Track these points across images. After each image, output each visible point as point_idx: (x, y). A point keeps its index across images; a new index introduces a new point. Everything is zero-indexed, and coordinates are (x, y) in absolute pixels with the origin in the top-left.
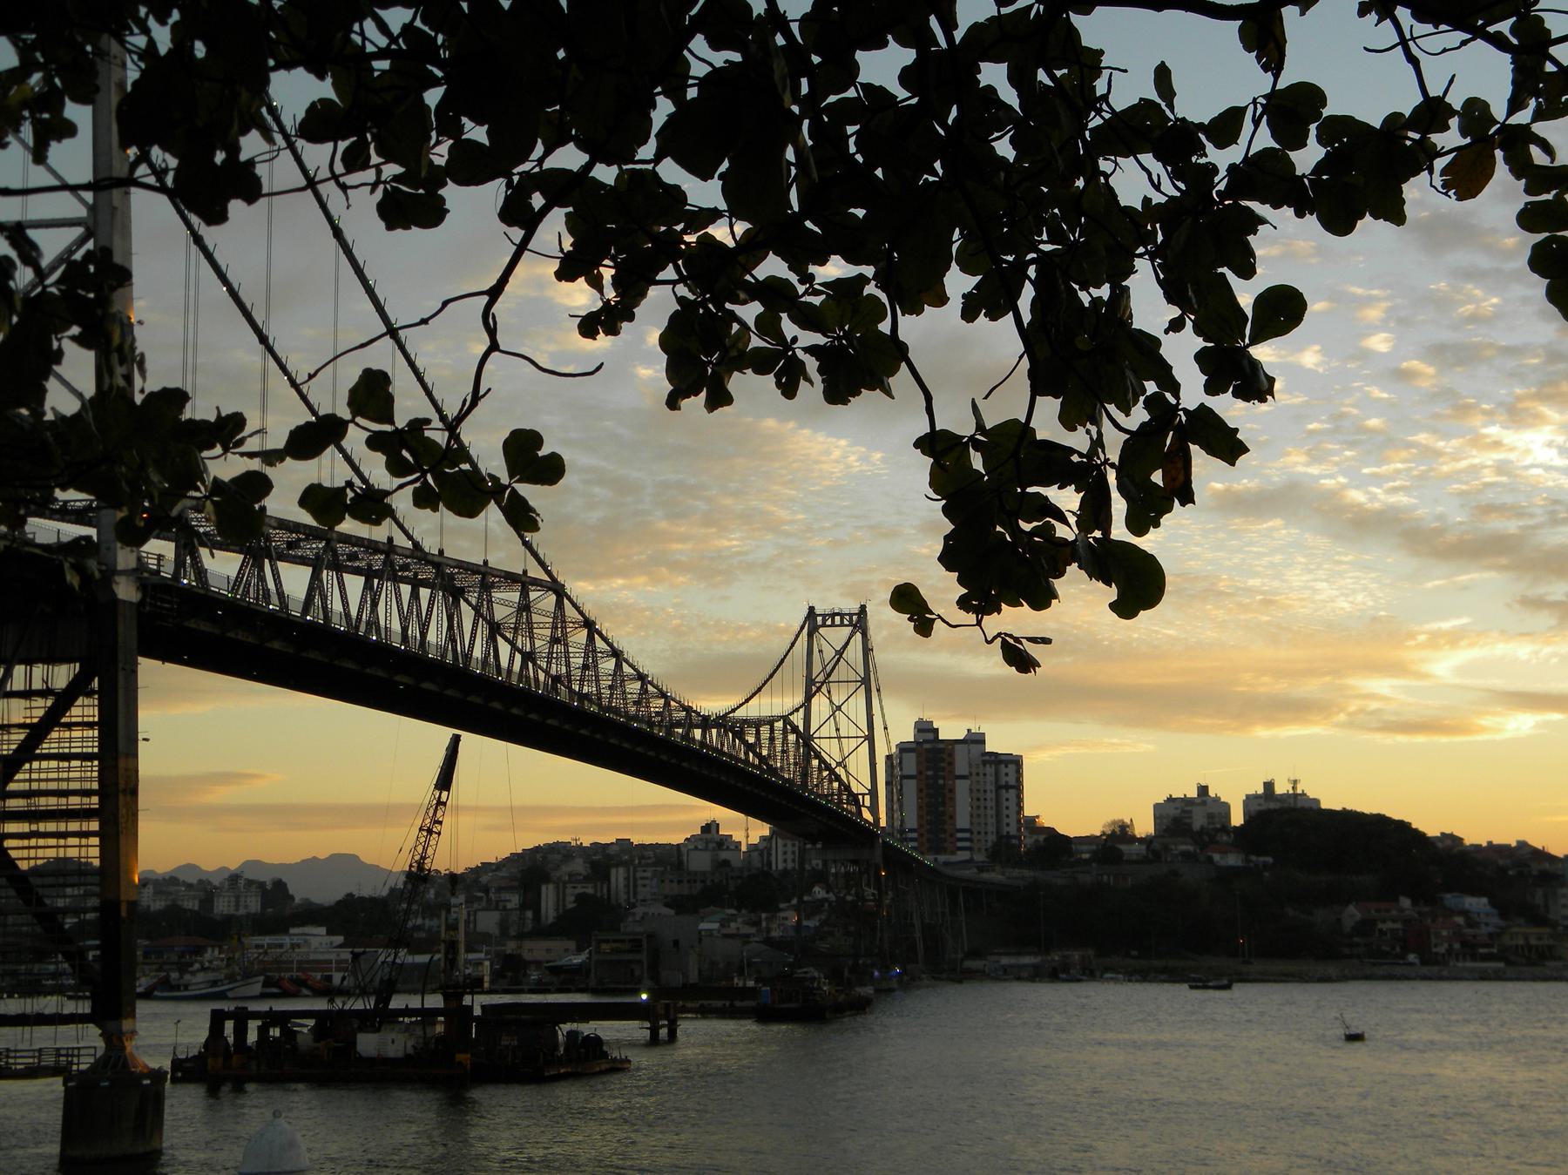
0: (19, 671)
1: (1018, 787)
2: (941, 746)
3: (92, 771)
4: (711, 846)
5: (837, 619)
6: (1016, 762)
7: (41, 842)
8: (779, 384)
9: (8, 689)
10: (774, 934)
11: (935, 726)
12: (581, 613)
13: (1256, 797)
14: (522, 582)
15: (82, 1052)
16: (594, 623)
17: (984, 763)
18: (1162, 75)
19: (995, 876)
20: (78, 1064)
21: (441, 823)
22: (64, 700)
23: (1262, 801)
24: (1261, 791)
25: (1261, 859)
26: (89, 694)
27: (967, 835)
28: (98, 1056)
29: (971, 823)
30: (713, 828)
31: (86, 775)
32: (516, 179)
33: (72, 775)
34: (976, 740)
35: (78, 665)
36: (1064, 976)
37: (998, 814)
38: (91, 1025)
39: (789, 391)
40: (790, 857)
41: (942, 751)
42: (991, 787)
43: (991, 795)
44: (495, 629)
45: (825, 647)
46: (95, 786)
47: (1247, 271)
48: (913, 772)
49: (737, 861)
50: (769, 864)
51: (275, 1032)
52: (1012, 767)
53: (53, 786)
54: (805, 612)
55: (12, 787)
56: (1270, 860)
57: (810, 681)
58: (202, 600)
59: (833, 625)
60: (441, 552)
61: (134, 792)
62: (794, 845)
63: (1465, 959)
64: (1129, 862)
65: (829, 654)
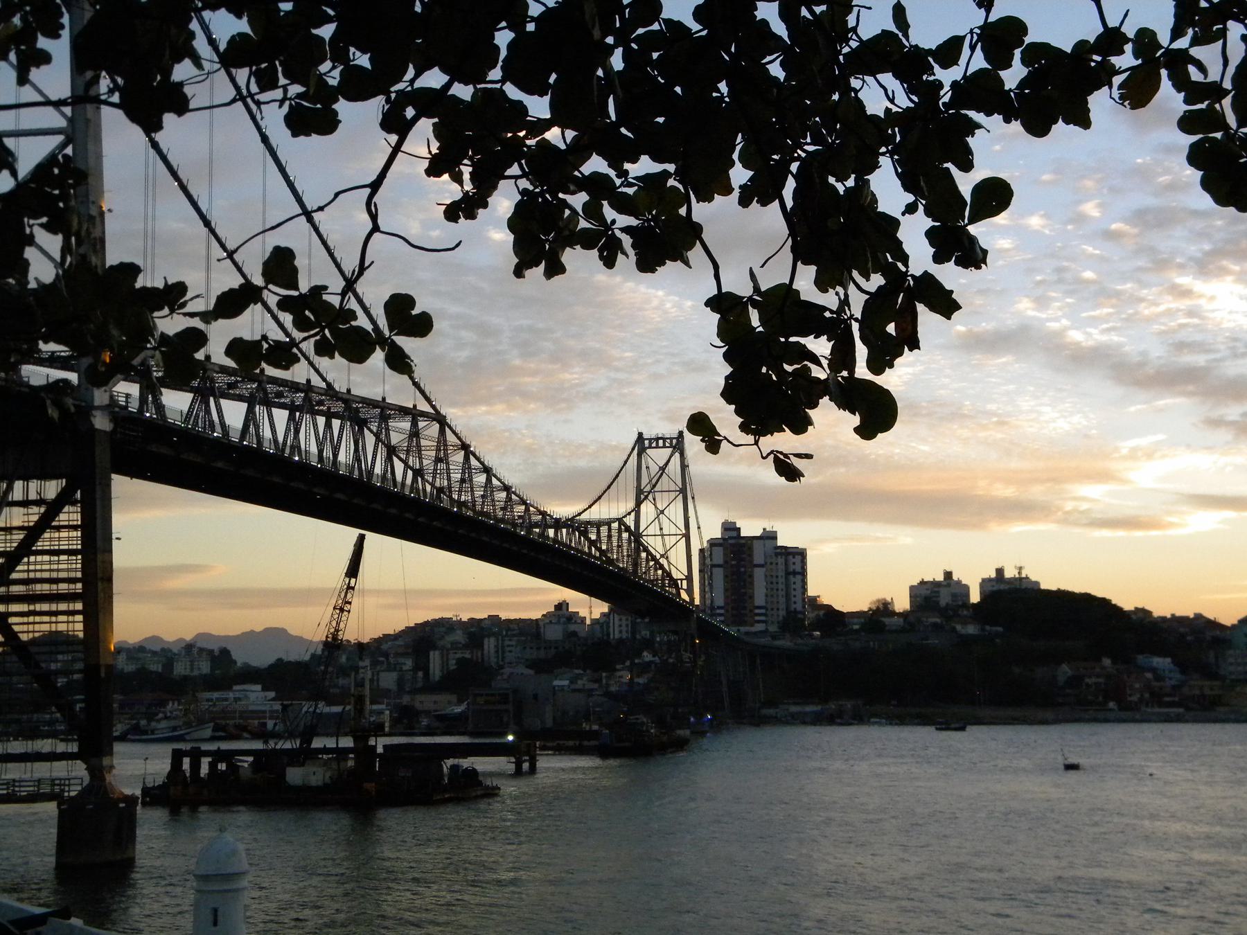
0: (18, 485)
1: (803, 573)
2: (743, 541)
3: (76, 563)
4: (563, 620)
5: (661, 442)
6: (801, 554)
7: (38, 619)
8: (601, 257)
9: (10, 499)
10: (613, 689)
11: (738, 526)
12: (459, 438)
13: (990, 580)
14: (413, 414)
15: (72, 782)
16: (469, 446)
17: (777, 555)
18: (899, 13)
19: (786, 643)
20: (69, 791)
21: (350, 603)
22: (54, 508)
23: (994, 583)
24: (993, 575)
25: (994, 629)
26: (74, 503)
27: (763, 611)
28: (85, 784)
29: (766, 602)
30: (564, 607)
31: (72, 566)
32: (393, 96)
33: (61, 567)
34: (770, 536)
35: (64, 480)
36: (839, 721)
37: (787, 596)
38: (78, 762)
39: (609, 262)
40: (624, 628)
41: (743, 545)
42: (781, 573)
43: (781, 580)
44: (392, 451)
45: (651, 463)
46: (79, 575)
47: (967, 166)
48: (721, 562)
49: (582, 634)
50: (608, 635)
51: (222, 766)
52: (798, 558)
53: (46, 575)
54: (635, 436)
55: (14, 576)
56: (1000, 629)
57: (639, 491)
58: (161, 429)
59: (657, 447)
60: (349, 391)
61: (109, 580)
62: (627, 620)
63: (1153, 706)
64: (891, 632)
65: (654, 469)
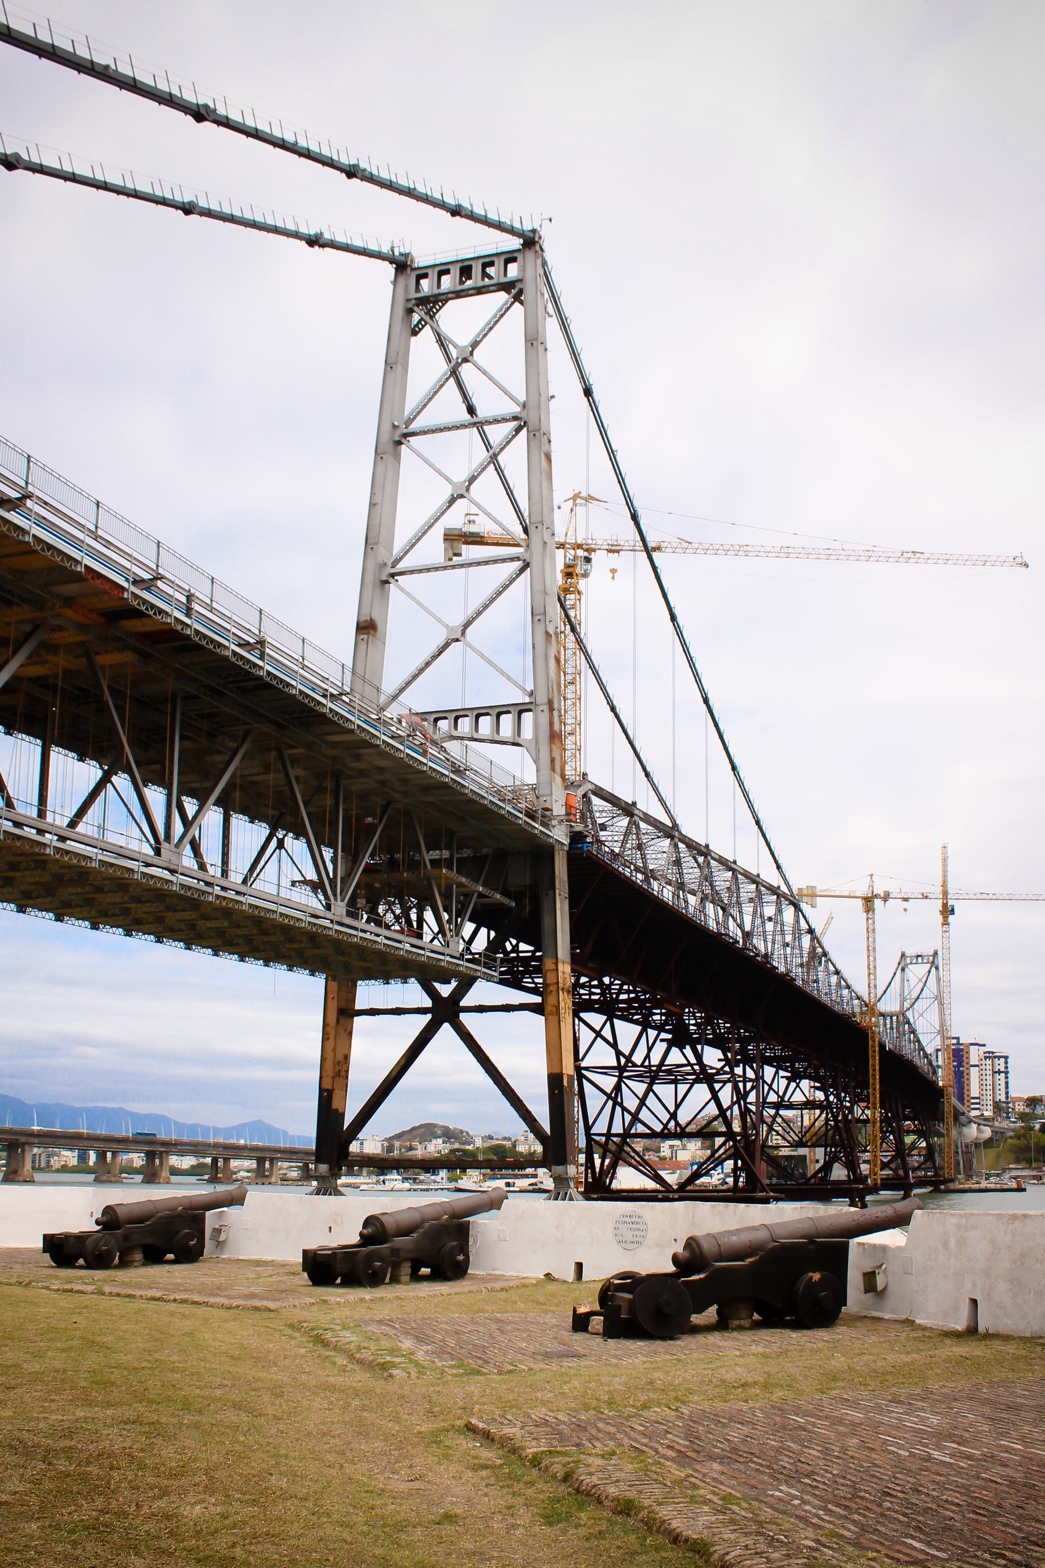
2: (962, 1047)
17: (986, 1058)
43: (989, 1078)
52: (1002, 1060)
